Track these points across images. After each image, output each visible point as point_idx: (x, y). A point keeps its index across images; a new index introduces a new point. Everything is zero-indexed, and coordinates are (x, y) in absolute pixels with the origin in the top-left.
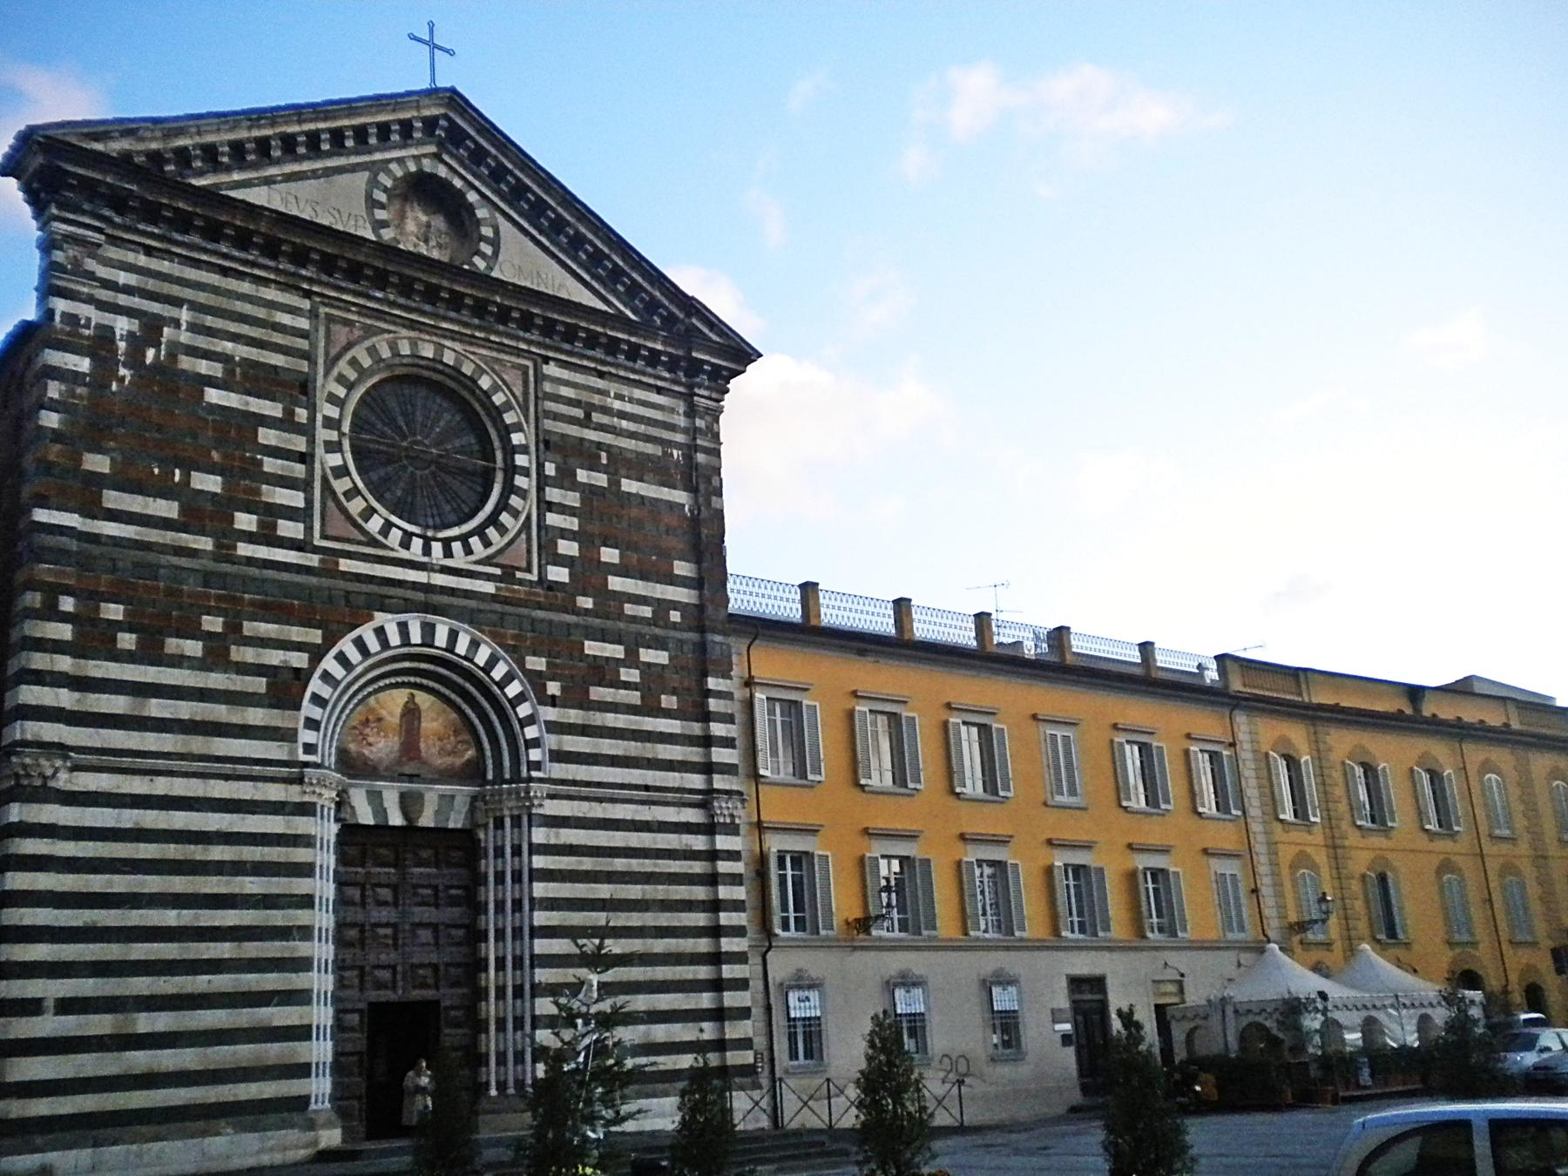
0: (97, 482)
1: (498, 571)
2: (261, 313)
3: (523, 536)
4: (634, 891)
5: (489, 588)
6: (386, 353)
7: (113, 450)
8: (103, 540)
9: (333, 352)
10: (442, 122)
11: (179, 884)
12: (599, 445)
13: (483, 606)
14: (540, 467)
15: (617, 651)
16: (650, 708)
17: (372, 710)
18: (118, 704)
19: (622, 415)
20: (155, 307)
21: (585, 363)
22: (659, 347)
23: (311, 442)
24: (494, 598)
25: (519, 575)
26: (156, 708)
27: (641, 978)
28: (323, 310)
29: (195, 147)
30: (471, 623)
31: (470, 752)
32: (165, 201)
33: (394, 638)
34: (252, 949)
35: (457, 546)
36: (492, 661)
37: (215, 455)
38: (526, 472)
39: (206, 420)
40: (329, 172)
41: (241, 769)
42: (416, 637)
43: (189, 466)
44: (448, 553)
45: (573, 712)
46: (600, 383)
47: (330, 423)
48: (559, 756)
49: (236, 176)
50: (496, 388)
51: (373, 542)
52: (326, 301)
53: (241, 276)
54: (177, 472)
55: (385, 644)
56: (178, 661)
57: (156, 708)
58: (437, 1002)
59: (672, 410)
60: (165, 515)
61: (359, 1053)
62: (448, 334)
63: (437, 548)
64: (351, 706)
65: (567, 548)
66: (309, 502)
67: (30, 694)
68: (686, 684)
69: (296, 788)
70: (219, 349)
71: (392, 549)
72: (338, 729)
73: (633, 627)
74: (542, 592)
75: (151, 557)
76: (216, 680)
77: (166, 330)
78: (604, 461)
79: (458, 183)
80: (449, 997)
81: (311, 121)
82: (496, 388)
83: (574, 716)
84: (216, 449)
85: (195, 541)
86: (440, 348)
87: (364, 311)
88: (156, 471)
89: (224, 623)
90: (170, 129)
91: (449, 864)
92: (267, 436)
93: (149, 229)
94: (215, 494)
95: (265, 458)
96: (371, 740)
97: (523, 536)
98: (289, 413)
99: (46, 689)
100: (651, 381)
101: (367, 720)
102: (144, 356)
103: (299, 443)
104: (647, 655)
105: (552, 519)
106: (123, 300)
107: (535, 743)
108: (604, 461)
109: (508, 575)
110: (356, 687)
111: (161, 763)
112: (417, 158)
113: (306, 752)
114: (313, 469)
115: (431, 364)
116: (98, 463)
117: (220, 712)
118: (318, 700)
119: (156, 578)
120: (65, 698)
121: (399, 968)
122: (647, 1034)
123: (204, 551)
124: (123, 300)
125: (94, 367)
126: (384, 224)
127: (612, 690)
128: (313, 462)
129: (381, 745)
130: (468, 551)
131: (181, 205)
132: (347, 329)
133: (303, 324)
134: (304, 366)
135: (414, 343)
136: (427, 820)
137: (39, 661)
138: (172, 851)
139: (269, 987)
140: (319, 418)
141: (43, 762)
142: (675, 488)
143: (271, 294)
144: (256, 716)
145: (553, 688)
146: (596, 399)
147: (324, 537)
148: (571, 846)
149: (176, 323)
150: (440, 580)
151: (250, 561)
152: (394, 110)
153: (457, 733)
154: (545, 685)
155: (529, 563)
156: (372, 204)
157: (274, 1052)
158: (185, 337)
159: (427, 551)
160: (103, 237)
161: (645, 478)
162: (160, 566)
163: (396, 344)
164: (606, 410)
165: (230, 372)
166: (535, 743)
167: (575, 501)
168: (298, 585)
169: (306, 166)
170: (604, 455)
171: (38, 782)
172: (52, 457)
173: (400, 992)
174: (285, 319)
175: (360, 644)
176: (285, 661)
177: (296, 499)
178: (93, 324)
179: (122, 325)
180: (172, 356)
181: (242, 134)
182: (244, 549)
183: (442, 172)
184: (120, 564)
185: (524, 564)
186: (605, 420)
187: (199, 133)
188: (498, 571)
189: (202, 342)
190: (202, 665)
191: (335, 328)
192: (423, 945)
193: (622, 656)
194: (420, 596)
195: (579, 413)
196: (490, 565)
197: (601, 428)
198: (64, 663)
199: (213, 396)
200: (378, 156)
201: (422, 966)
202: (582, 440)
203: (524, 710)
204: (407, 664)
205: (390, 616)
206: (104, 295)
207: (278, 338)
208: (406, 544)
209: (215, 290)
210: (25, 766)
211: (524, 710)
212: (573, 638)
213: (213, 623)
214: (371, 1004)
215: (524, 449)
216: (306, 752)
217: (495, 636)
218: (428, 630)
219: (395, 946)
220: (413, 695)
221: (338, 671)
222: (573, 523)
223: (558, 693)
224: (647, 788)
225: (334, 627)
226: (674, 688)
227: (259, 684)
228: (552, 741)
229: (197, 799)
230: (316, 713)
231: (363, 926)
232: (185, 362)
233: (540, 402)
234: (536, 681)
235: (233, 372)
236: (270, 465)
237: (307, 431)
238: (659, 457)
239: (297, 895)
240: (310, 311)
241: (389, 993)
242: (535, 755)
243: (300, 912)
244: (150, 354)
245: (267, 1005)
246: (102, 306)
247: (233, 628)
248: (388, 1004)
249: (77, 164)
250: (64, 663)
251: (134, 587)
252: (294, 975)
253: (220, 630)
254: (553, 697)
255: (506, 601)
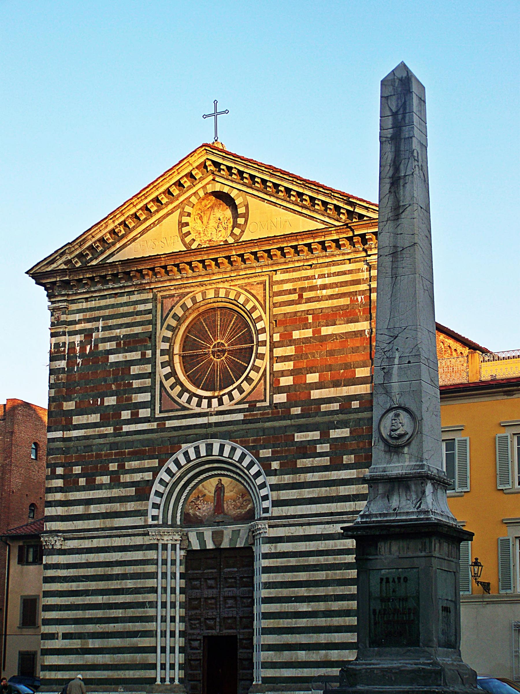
0: (70, 413)
1: (247, 406)
2: (131, 309)
3: (262, 381)
4: (321, 575)
5: (240, 417)
6: (189, 304)
7: (75, 398)
8: (73, 439)
9: (164, 315)
10: (208, 163)
11: (102, 585)
12: (307, 312)
13: (235, 428)
14: (271, 337)
15: (315, 435)
16: (337, 466)
17: (201, 492)
18: (79, 510)
19: (324, 287)
20: (89, 326)
21: (297, 264)
22: (335, 237)
23: (154, 367)
24: (244, 422)
25: (258, 405)
26: (93, 509)
27: (324, 624)
28: (159, 295)
29: (95, 243)
30: (230, 439)
31: (249, 505)
32: (82, 277)
33: (193, 456)
34: (130, 612)
35: (226, 398)
36: (243, 456)
37: (113, 387)
38: (264, 344)
39: (110, 371)
40: (160, 220)
41: (124, 532)
42: (203, 453)
43: (103, 396)
44: (221, 403)
45: (286, 477)
46: (309, 273)
47: (163, 352)
48: (277, 503)
49: (118, 246)
50: (247, 301)
51: (184, 408)
52: (159, 289)
53: (122, 294)
54: (99, 399)
55: (189, 460)
56: (100, 487)
57: (93, 509)
58: (236, 636)
59: (358, 270)
60: (95, 421)
61: (200, 660)
62: (220, 280)
63: (215, 402)
64: (187, 491)
65: (286, 381)
66: (153, 397)
67: (49, 511)
68: (361, 445)
69: (147, 537)
70: (114, 335)
71: (192, 409)
72: (181, 504)
73: (327, 418)
74: (270, 411)
75: (89, 442)
76: (116, 492)
77: (94, 334)
78: (310, 321)
79: (226, 190)
80: (240, 633)
81: (140, 202)
82: (247, 301)
83: (287, 479)
84: (114, 384)
85: (106, 430)
86: (217, 291)
87: (177, 286)
88: (91, 402)
89: (118, 465)
90: (80, 242)
91: (243, 566)
92: (135, 370)
93: (82, 291)
94: (113, 405)
95: (134, 381)
96: (200, 506)
97: (262, 381)
98: (143, 354)
99: (53, 508)
100: (341, 258)
101: (198, 497)
102: (86, 350)
103: (148, 368)
104: (334, 434)
105: (278, 367)
106: (78, 327)
107: (265, 498)
108: (310, 321)
109: (252, 406)
110: (182, 483)
111: (95, 533)
112: (204, 187)
113: (152, 520)
114: (155, 379)
115: (215, 300)
116: (69, 406)
117: (117, 507)
118: (158, 494)
119: (92, 451)
120: (60, 511)
121: (218, 620)
122: (326, 655)
123: (110, 433)
124: (78, 327)
125: (67, 363)
126: (189, 233)
127: (311, 459)
128: (155, 375)
129: (204, 509)
130: (231, 398)
131: (88, 276)
132: (171, 299)
133: (149, 306)
134: (150, 328)
135: (204, 294)
136: (225, 544)
137: (50, 497)
138: (100, 571)
139: (136, 629)
140: (158, 352)
141: (51, 538)
142: (357, 321)
143: (135, 297)
144: (131, 506)
145: (275, 465)
146: (306, 284)
147: (161, 412)
148: (284, 553)
149: (98, 329)
150: (214, 419)
151: (128, 433)
152: (178, 173)
153: (243, 496)
154: (271, 464)
155: (265, 396)
156: (182, 225)
157: (139, 657)
158: (101, 335)
159: (210, 405)
160: (65, 304)
161: (337, 322)
162: (94, 445)
163: (195, 297)
164: (312, 288)
165: (118, 345)
166: (265, 498)
167: (292, 352)
168: (147, 440)
169: (148, 223)
170: (310, 317)
171: (50, 547)
172: (52, 409)
173: (218, 631)
174: (141, 307)
175: (177, 462)
176: (143, 478)
177: (146, 397)
178: (67, 343)
179: (78, 339)
180: (96, 346)
181: (111, 227)
182: (126, 428)
183: (218, 187)
184: (79, 448)
185: (263, 398)
186: (312, 294)
187: (93, 237)
188: (247, 406)
189: (107, 334)
190: (110, 487)
191: (165, 301)
192: (229, 608)
193: (319, 438)
194: (203, 431)
195: (295, 297)
196: (244, 403)
197: (309, 300)
198: (59, 496)
199: (112, 358)
200: (181, 199)
201: (228, 618)
202: (296, 312)
203: (260, 481)
204: (207, 466)
205: (189, 445)
206: (71, 328)
207: (138, 319)
208: (199, 405)
209: (113, 306)
210: (46, 541)
211: (260, 481)
212: (287, 434)
213: (113, 467)
214: (204, 637)
215: (263, 330)
216: (152, 520)
217: (242, 443)
218: (210, 447)
219: (216, 609)
220: (220, 480)
221: (166, 478)
222: (289, 365)
223: (278, 468)
224: (332, 514)
225: (163, 457)
226: (353, 450)
227: (131, 491)
228: (274, 495)
229: (108, 547)
230: (157, 500)
231: (200, 598)
232: (102, 347)
233: (271, 299)
234: (265, 463)
235: (120, 342)
236: (136, 383)
237: (152, 361)
238: (348, 305)
239: (148, 587)
240: (152, 298)
241: (214, 631)
242: (266, 504)
243: (149, 595)
244: (88, 348)
245: (137, 637)
246: (71, 333)
247: (121, 466)
248: (212, 636)
249: (47, 278)
250: (59, 496)
251: (85, 455)
252: (147, 624)
253: (116, 469)
254: (276, 470)
255: (250, 422)
